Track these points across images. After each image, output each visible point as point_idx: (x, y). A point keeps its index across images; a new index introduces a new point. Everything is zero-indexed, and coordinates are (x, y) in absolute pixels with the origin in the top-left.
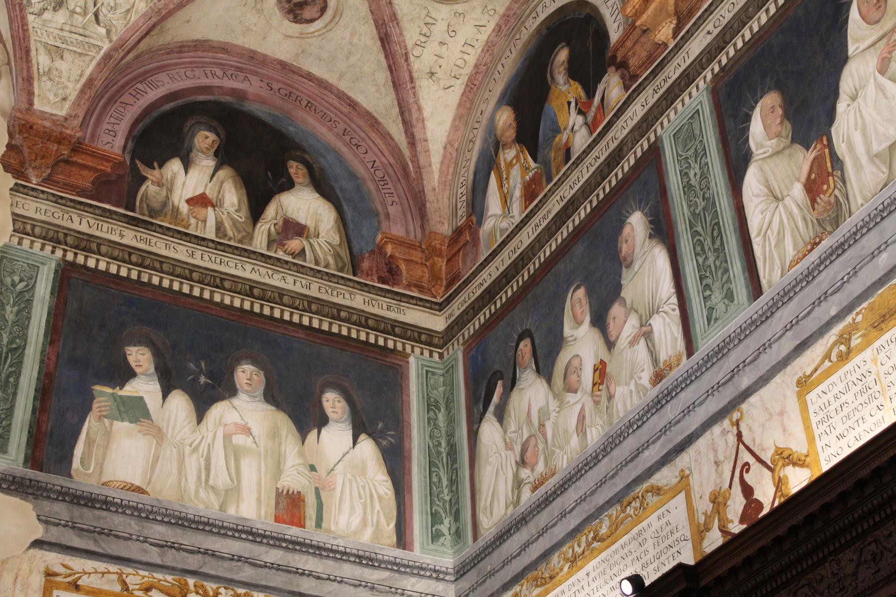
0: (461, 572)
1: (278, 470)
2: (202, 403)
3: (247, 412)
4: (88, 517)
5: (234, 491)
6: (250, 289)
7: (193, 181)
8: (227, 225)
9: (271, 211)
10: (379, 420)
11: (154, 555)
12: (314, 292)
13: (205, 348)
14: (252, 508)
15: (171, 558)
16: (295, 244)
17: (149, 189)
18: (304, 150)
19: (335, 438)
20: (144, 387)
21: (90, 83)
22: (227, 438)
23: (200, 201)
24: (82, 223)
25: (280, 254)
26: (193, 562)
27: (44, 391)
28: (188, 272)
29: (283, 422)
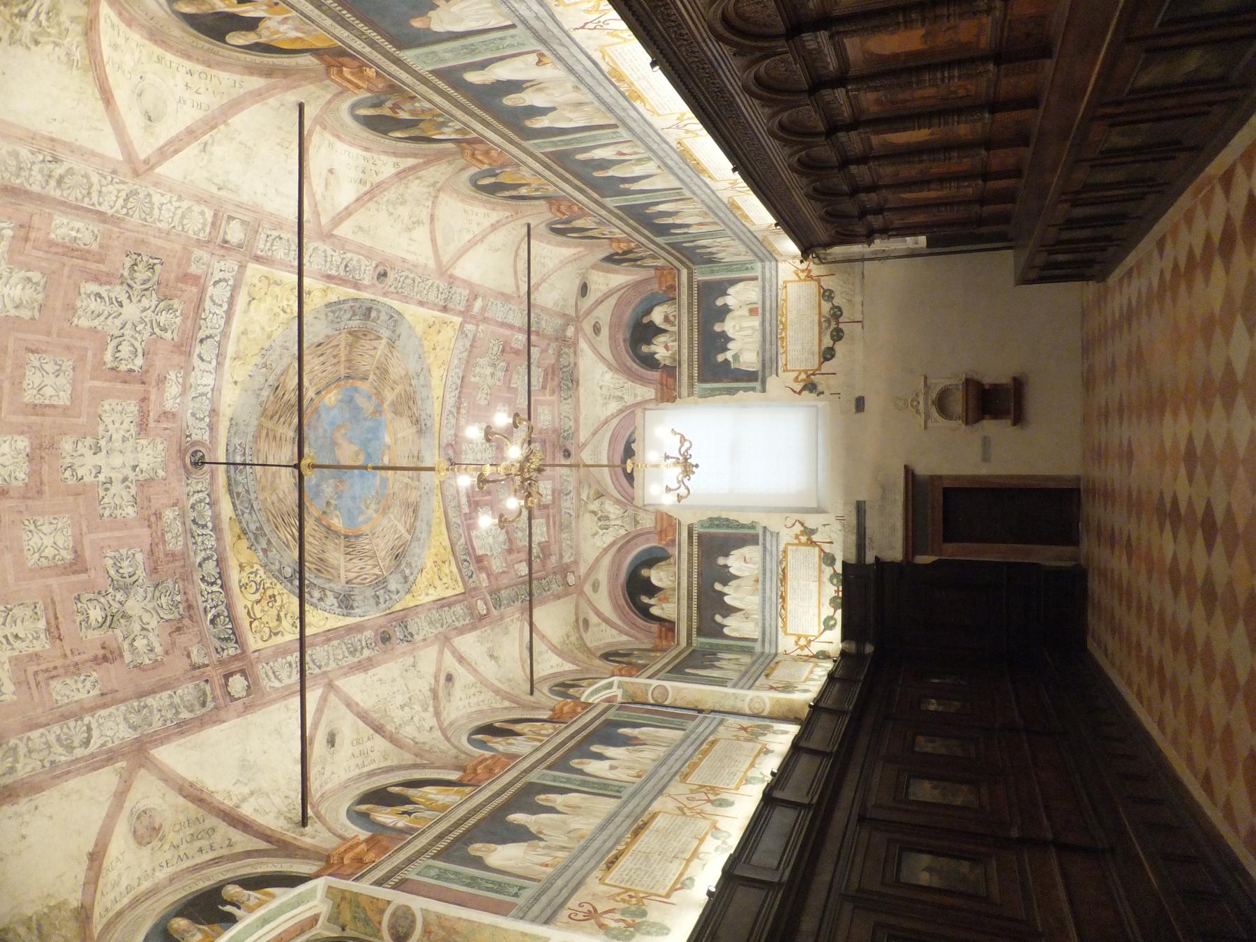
0: (762, 261)
2: (729, 339)
3: (729, 326)
4: (768, 365)
5: (752, 328)
6: (691, 330)
10: (721, 288)
13: (711, 343)
14: (756, 322)
16: (672, 318)
17: (667, 362)
19: (730, 300)
20: (729, 355)
23: (667, 347)
24: (685, 379)
27: (737, 381)
29: (729, 317)
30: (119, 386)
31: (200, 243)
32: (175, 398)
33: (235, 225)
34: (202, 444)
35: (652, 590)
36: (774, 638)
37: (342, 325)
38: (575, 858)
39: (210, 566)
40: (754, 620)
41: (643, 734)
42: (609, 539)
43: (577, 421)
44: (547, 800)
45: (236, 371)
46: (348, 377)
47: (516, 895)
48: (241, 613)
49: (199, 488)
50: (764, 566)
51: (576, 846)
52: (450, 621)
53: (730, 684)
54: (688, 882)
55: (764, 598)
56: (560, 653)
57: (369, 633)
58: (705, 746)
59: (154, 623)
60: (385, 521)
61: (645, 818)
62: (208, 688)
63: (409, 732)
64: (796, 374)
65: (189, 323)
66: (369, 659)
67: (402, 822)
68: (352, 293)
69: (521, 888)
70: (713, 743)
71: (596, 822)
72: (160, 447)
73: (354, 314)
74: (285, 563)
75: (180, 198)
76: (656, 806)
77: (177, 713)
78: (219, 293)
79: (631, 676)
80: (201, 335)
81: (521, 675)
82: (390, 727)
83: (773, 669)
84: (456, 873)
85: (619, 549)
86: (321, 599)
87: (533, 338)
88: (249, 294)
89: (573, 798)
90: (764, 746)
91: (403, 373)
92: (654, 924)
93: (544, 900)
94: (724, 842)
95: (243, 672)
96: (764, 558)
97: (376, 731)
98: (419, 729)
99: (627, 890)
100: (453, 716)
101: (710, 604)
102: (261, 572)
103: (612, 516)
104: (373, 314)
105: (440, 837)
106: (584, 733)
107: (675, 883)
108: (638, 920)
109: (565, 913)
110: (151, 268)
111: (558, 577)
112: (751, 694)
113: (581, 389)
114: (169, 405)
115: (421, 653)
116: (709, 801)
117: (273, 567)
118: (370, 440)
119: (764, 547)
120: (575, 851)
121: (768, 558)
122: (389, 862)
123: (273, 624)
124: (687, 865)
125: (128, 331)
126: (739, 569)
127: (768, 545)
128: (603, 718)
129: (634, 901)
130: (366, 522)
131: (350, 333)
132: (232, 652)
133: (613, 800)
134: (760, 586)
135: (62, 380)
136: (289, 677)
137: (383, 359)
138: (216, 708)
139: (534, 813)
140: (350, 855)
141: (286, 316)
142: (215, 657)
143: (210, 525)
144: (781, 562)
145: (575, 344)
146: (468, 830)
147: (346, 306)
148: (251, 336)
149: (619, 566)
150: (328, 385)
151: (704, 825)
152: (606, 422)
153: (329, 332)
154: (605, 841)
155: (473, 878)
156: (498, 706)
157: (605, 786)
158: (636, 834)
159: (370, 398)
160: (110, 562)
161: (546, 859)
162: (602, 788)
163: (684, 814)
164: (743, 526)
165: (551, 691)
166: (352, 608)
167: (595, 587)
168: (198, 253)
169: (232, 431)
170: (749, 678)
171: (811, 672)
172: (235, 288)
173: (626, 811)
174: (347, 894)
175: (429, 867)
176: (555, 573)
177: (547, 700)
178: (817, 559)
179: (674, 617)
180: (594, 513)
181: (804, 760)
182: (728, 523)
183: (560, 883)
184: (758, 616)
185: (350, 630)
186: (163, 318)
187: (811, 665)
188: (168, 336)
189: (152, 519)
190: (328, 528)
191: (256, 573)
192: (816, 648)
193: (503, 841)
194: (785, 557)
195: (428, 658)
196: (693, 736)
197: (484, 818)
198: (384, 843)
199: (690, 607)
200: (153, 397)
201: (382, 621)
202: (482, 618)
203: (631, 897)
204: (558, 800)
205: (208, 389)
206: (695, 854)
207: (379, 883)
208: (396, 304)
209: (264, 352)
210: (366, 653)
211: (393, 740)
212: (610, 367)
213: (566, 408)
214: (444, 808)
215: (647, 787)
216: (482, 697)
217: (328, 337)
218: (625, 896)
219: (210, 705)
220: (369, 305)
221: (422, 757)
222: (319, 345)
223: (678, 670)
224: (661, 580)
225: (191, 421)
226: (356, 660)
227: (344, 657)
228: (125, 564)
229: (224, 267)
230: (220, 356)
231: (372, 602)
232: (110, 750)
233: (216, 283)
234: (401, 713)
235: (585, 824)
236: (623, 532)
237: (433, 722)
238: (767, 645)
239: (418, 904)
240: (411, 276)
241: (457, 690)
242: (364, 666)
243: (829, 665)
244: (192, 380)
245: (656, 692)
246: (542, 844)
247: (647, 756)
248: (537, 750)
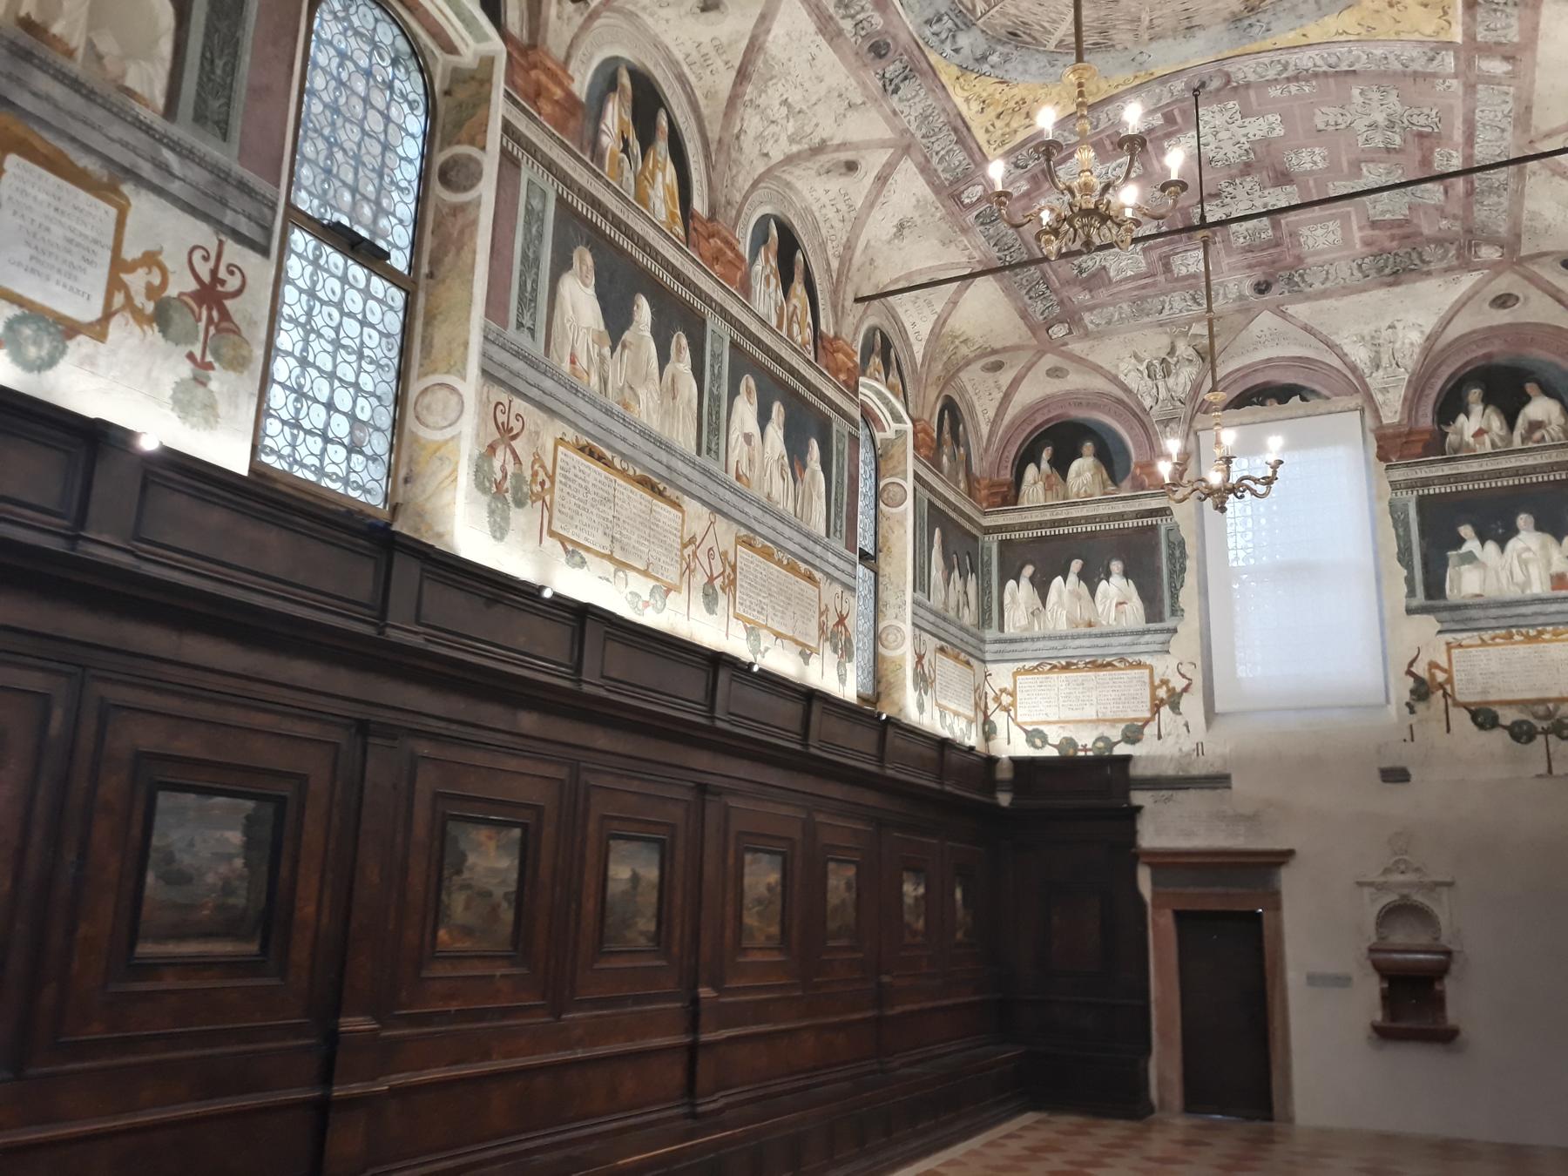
1: (1549, 563)
3: (1528, 540)
6: (1516, 472)
7: (1476, 423)
8: (1497, 440)
9: (1521, 422)
11: (1493, 623)
12: (1554, 459)
15: (1502, 622)
16: (1537, 435)
17: (1452, 438)
18: (1532, 373)
20: (1472, 545)
21: (1405, 399)
22: (1519, 556)
23: (1480, 433)
25: (1531, 445)
26: (1513, 622)
28: (1481, 476)
29: (1548, 538)
35: (1061, 465)
36: (1007, 656)
38: (592, 402)
40: (1031, 624)
41: (814, 473)
42: (1133, 381)
43: (1324, 294)
44: (679, 351)
47: (520, 325)
50: (1113, 634)
51: (612, 401)
52: (936, 147)
53: (921, 596)
54: (577, 559)
55: (1066, 637)
56: (936, 334)
57: (878, 21)
58: (803, 568)
61: (670, 492)
63: (752, 123)
64: (1445, 665)
66: (840, 32)
67: (609, 142)
69: (532, 331)
70: (810, 578)
71: (655, 424)
76: (691, 506)
79: (915, 447)
81: (885, 278)
82: (750, 91)
83: (956, 658)
84: (540, 235)
85: (1120, 401)
87: (1460, 184)
89: (689, 387)
90: (813, 651)
92: (506, 519)
93: (519, 365)
94: (646, 604)
96: (1126, 634)
97: (739, 72)
98: (760, 137)
99: (552, 478)
100: (799, 185)
101: (1046, 556)
103: (1171, 381)
105: (595, 203)
106: (802, 390)
107: (573, 542)
108: (509, 496)
109: (504, 397)
111: (1057, 310)
112: (907, 628)
113: (1382, 293)
115: (874, 114)
116: (711, 579)
119: (1143, 633)
120: (601, 399)
121: (1127, 639)
122: (543, 135)
124: (603, 556)
126: (1105, 596)
127: (1147, 638)
128: (832, 414)
129: (539, 488)
133: (693, 443)
134: (1083, 630)
139: (656, 333)
140: (543, 78)
144: (1122, 660)
145: (1466, 266)
146: (611, 242)
149: (1096, 407)
151: (672, 575)
152: (1331, 346)
154: (624, 440)
155: (537, 260)
156: (830, 253)
157: (715, 430)
158: (644, 483)
161: (583, 361)
162: (711, 426)
163: (685, 546)
164: (1174, 596)
165: (873, 330)
167: (1055, 373)
170: (933, 623)
171: (957, 714)
173: (680, 466)
174: (487, 86)
175: (544, 195)
176: (1061, 303)
177: (853, 328)
178: (1132, 715)
179: (1025, 502)
180: (1172, 352)
181: (790, 711)
182: (1178, 571)
183: (548, 384)
184: (1036, 630)
187: (971, 714)
192: (999, 719)
193: (601, 296)
194: (1132, 666)
195: (868, 127)
196: (818, 549)
197: (635, 262)
198: (572, 124)
199: (1041, 525)
201: (903, 37)
202: (956, 198)
203: (542, 484)
204: (682, 365)
206: (622, 566)
207: (508, 128)
210: (847, 25)
211: (733, 100)
212: (1432, 339)
213: (1344, 271)
214: (642, 198)
215: (721, 491)
216: (838, 225)
218: (541, 476)
221: (718, 150)
223: (934, 517)
224: (1078, 475)
226: (832, 10)
231: (929, 13)
234: (776, 103)
235: (647, 408)
236: (1148, 402)
237: (777, 156)
238: (997, 647)
239: (486, 190)
241: (836, 184)
242: (826, 27)
243: (973, 739)
245: (896, 489)
246: (607, 351)
247: (778, 487)
248: (763, 323)
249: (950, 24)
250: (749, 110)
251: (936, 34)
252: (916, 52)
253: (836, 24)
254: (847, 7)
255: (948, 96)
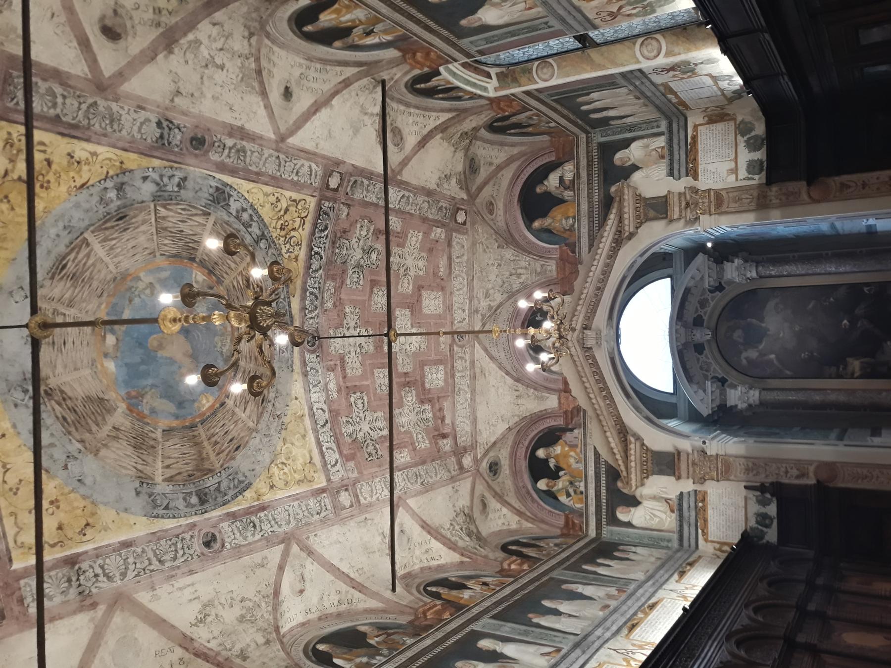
30: (357, 383)
31: (356, 482)
32: (330, 381)
33: (347, 504)
34: (309, 351)
37: (224, 475)
39: (315, 266)
45: (298, 406)
46: (192, 427)
48: (308, 226)
49: (311, 321)
57: (214, 157)
59: (354, 240)
60: (126, 264)
62: (349, 189)
65: (338, 431)
66: (230, 135)
68: (233, 508)
72: (332, 348)
73: (218, 489)
74: (264, 252)
75: (378, 498)
77: (368, 186)
78: (333, 457)
80: (329, 425)
86: (244, 210)
88: (314, 464)
91: (103, 452)
95: (328, 185)
102: (284, 251)
104: (194, 500)
110: (370, 454)
114: (332, 376)
115: (157, 97)
117: (274, 252)
118: (143, 362)
123: (293, 209)
125: (362, 415)
130: (160, 269)
131: (210, 471)
132: (327, 204)
135: (378, 382)
136: (303, 165)
137: (150, 459)
138: (351, 175)
141: (279, 461)
142: (336, 206)
143: (308, 294)
147: (231, 493)
148: (298, 436)
150: (214, 414)
153: (233, 464)
159: (153, 411)
160: (361, 282)
166: (217, 189)
168: (356, 475)
169: (290, 362)
172: (325, 464)
185: (233, 172)
186: (351, 429)
188: (345, 419)
189: (338, 304)
190: (211, 272)
191: (288, 251)
200: (341, 379)
201: (190, 160)
205: (313, 390)
208: (169, 524)
209: (283, 427)
210: (229, 142)
217: (233, 458)
219: (353, 179)
220: (207, 505)
222: (237, 449)
225: (318, 367)
227: (252, 152)
228: (355, 280)
229: (338, 474)
230: (312, 415)
231: (190, 184)
232: (399, 187)
233: (337, 462)
234: (228, 65)
240: (168, 564)
242: (241, 133)
244: (324, 394)
249: (169, 188)
250: (247, 52)
251: (170, 177)
252: (173, 158)
253: (236, 138)
254: (238, 151)
255: (114, 147)
